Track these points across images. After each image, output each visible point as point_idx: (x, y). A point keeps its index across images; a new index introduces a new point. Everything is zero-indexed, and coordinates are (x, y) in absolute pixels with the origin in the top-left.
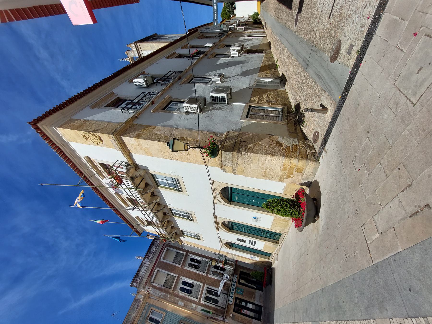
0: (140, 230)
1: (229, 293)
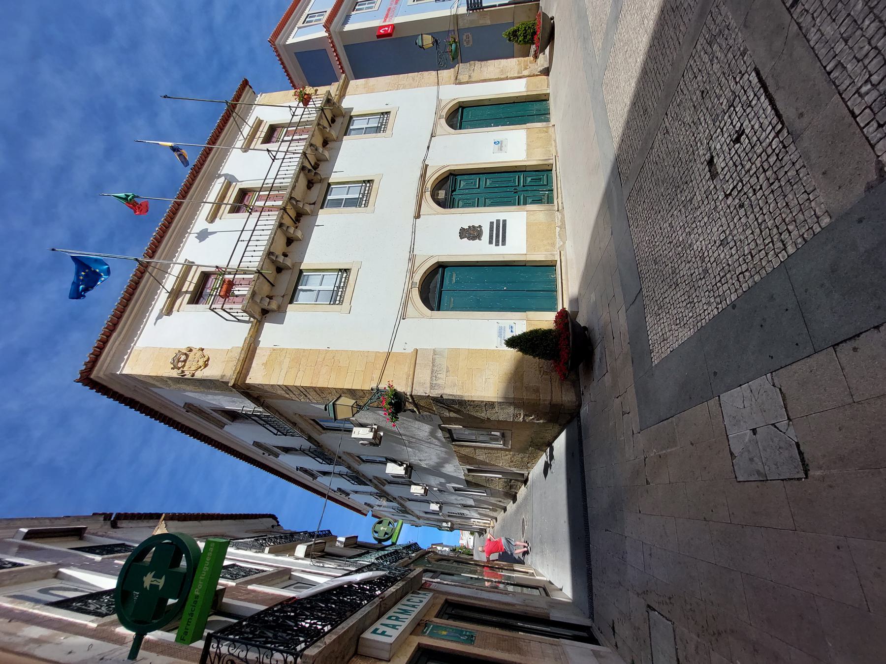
0: (106, 365)
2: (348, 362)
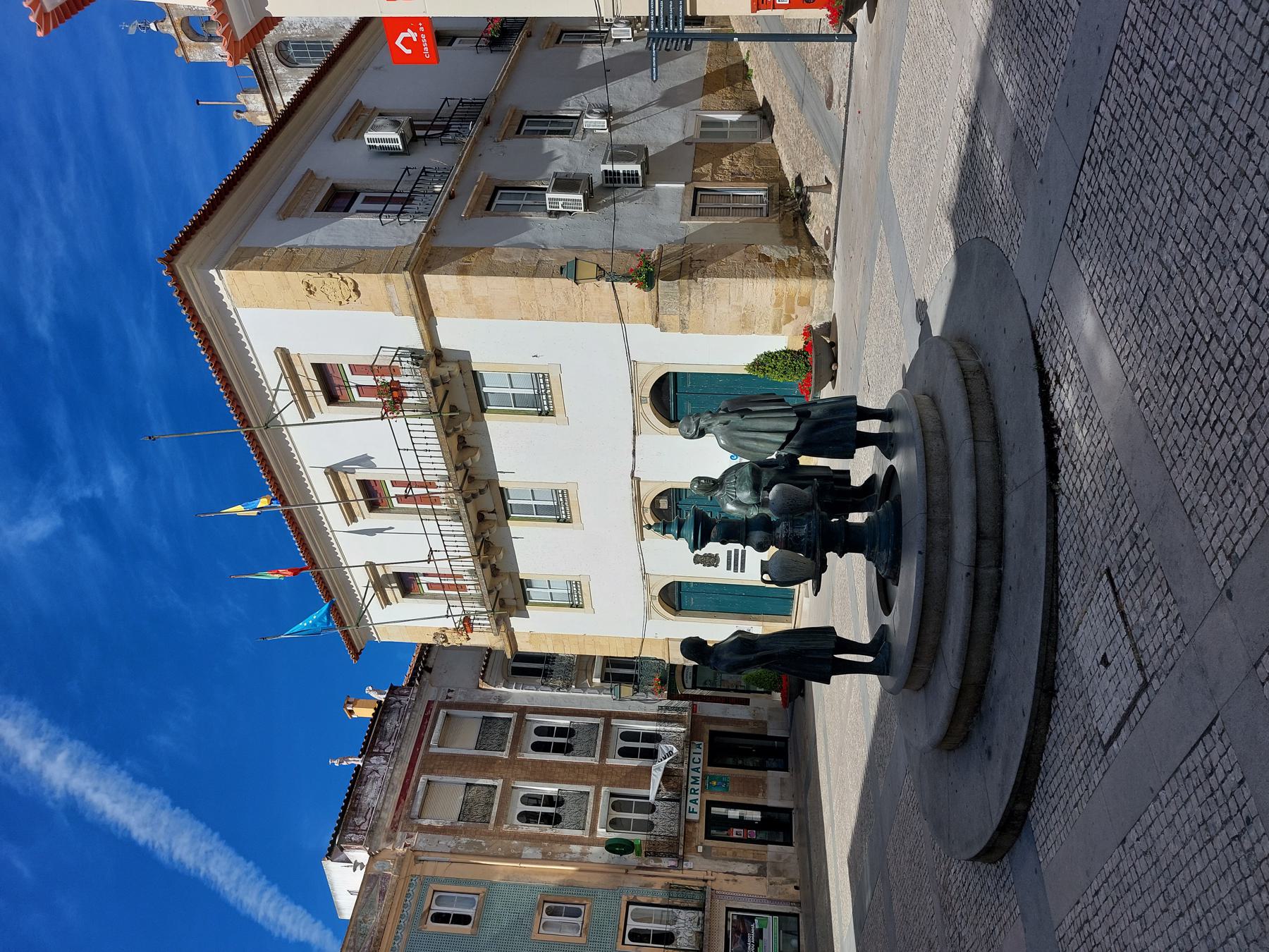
1: (684, 790)
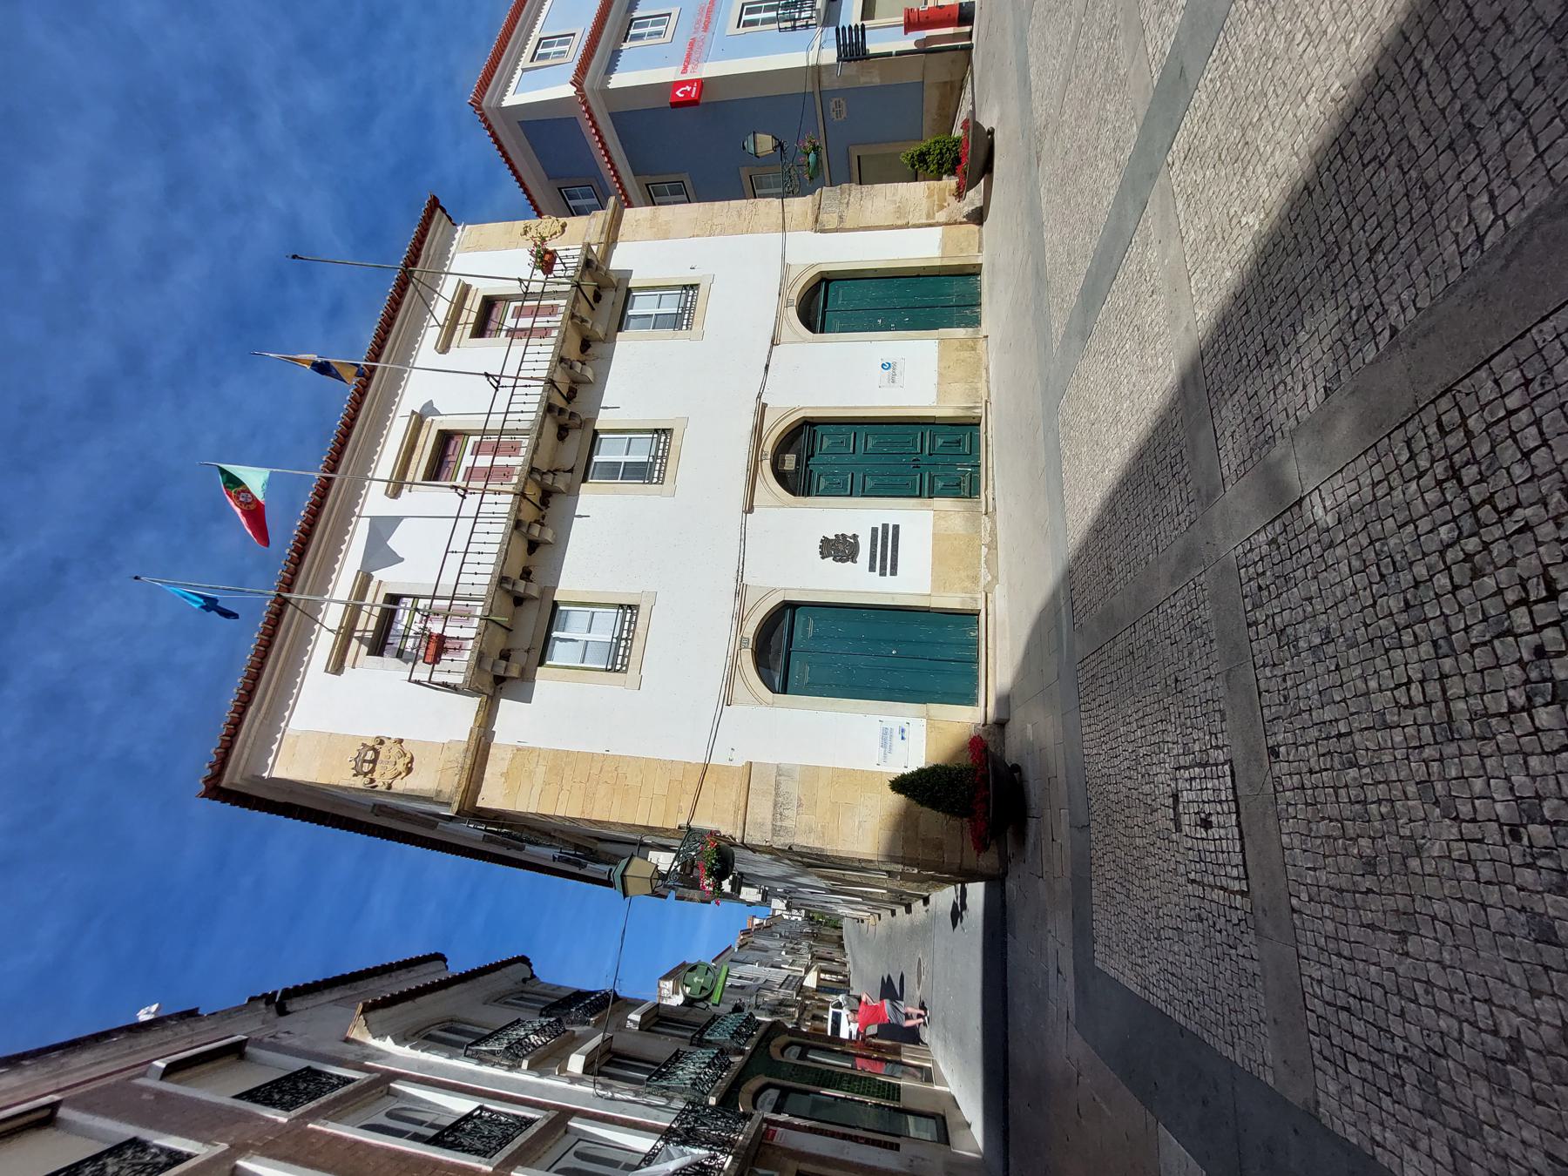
0: (243, 763)
2: (639, 779)
